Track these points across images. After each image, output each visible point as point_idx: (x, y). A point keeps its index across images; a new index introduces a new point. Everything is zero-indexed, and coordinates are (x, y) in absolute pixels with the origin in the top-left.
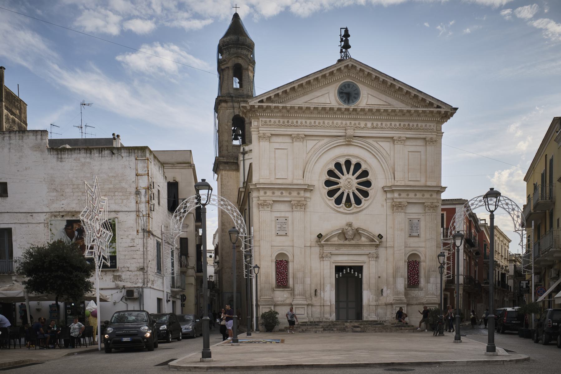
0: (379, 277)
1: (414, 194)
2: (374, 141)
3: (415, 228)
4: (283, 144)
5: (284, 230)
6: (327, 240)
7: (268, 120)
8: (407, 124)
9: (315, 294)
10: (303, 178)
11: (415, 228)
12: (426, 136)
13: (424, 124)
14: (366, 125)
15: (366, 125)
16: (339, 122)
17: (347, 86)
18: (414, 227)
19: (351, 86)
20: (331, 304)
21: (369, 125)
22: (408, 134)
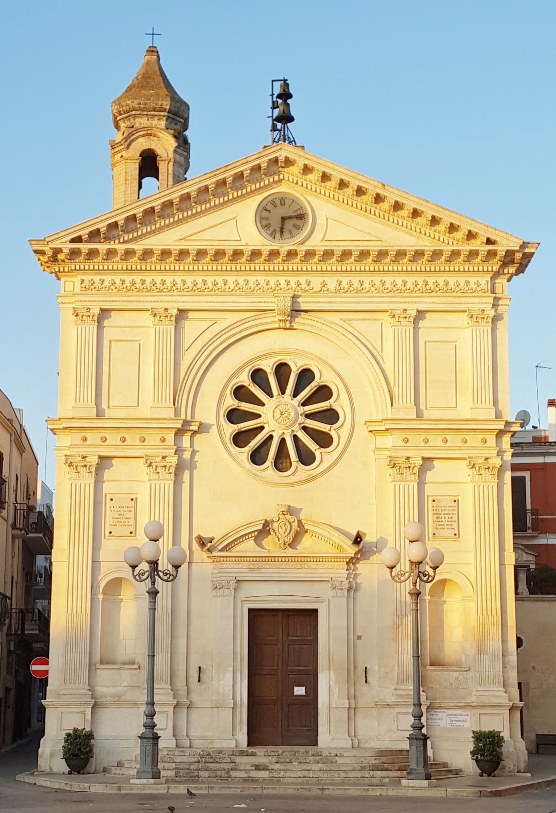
0: (359, 638)
1: (440, 439)
2: (344, 320)
3: (447, 519)
4: (131, 329)
5: (126, 524)
6: (226, 548)
7: (97, 278)
8: (420, 281)
9: (199, 677)
10: (174, 404)
11: (447, 519)
12: (468, 305)
13: (462, 280)
14: (324, 284)
15: (324, 284)
16: (262, 279)
17: (278, 202)
18: (443, 516)
19: (288, 202)
20: (235, 703)
21: (332, 282)
22: (422, 303)
